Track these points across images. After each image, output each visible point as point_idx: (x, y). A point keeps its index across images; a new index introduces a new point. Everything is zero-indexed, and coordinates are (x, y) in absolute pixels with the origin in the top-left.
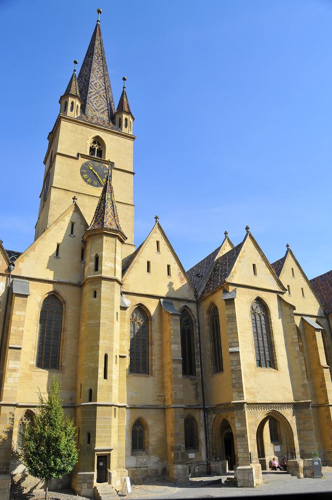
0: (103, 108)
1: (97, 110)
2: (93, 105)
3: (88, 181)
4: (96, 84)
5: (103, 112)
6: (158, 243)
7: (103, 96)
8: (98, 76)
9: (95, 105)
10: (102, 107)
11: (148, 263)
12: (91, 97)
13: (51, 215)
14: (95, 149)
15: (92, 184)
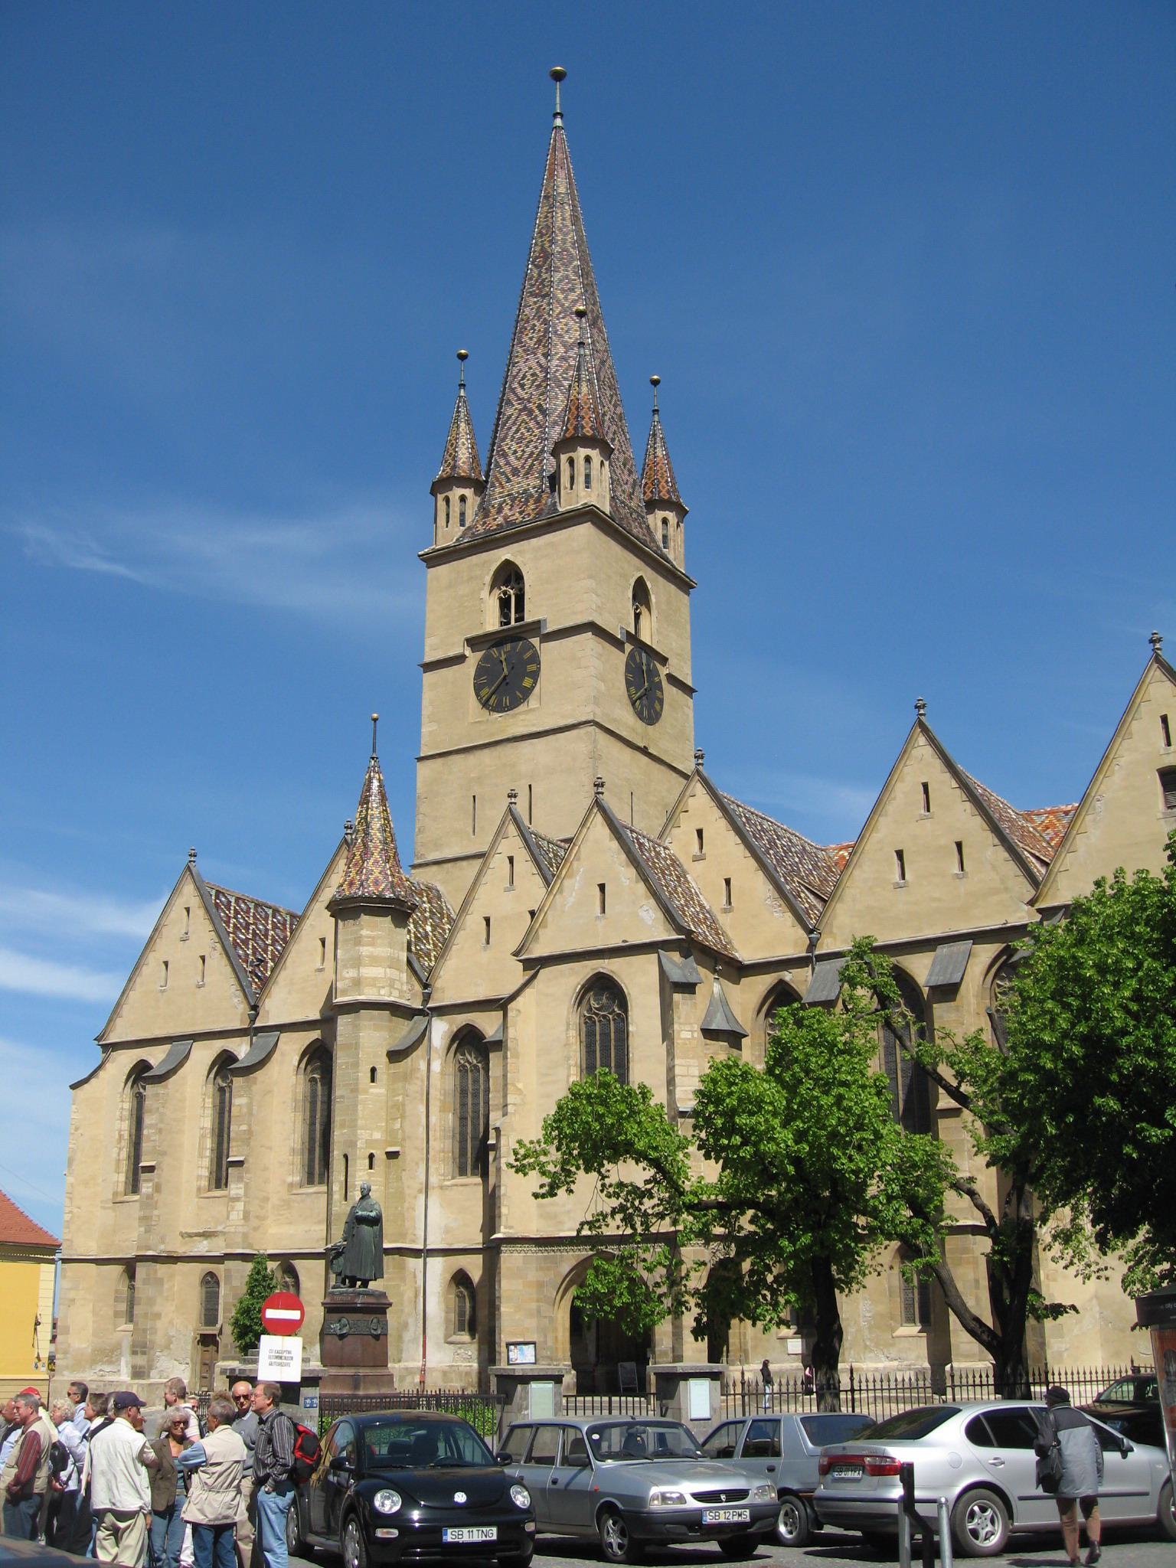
0: (532, 453)
1: (515, 472)
2: (508, 463)
3: (491, 702)
4: (523, 379)
5: (532, 465)
6: (511, 860)
7: (540, 407)
8: (532, 343)
9: (512, 458)
10: (528, 450)
11: (487, 920)
12: (503, 440)
13: (419, 830)
14: (510, 596)
15: (499, 708)
